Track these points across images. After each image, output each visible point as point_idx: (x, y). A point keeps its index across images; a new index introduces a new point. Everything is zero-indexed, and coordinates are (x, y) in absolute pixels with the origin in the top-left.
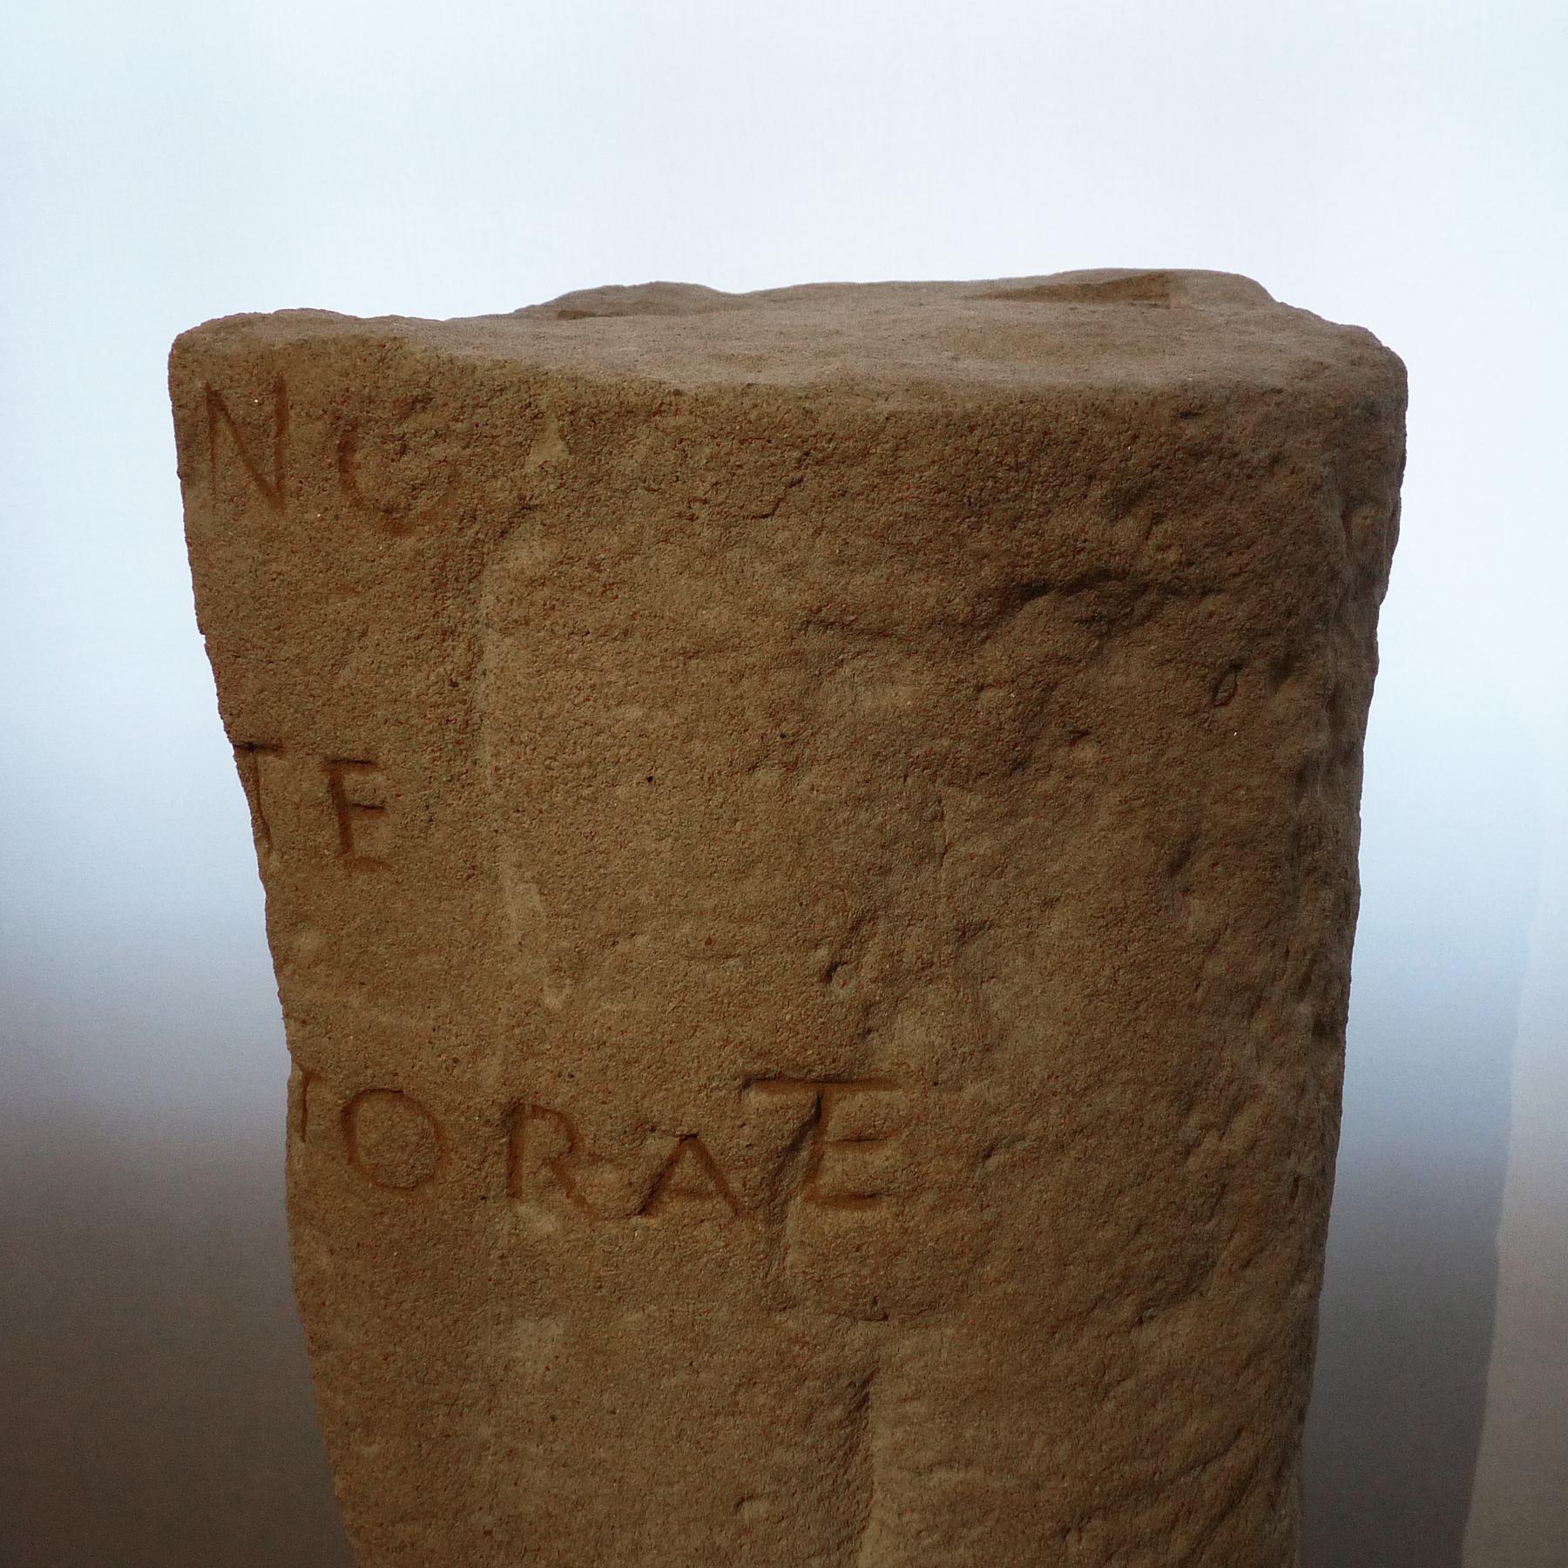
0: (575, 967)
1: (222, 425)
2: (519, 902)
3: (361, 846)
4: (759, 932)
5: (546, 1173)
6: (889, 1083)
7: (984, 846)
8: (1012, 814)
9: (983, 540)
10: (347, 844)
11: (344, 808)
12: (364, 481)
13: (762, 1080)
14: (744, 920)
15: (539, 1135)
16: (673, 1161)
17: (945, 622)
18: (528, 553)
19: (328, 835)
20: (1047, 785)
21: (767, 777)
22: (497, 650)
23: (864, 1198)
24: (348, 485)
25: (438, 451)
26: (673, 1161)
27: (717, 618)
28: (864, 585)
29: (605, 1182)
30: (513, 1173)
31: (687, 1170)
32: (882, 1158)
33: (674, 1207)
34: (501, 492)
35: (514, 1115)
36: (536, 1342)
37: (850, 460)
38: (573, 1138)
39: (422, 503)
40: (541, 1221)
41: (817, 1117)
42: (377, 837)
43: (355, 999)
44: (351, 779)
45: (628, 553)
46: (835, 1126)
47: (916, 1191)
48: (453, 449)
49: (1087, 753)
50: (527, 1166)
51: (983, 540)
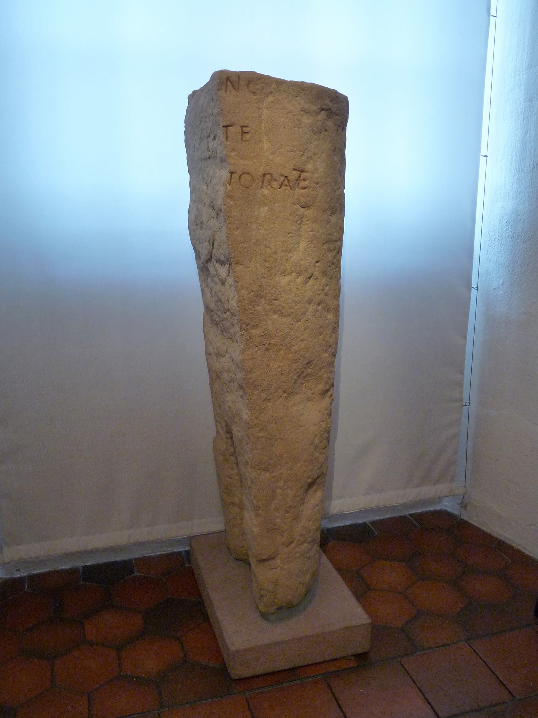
0: (273, 153)
1: (228, 81)
2: (266, 145)
3: (244, 138)
4: (295, 149)
5: (268, 183)
6: (307, 172)
7: (316, 143)
8: (319, 139)
9: (319, 102)
10: (242, 138)
11: (244, 133)
12: (250, 89)
13: (294, 170)
14: (294, 147)
15: (268, 177)
16: (284, 181)
17: (315, 111)
18: (271, 98)
19: (240, 137)
20: (323, 136)
21: (296, 129)
22: (265, 111)
23: (304, 188)
24: (248, 89)
25: (261, 85)
26: (284, 181)
27: (292, 108)
28: (307, 106)
29: (275, 184)
30: (262, 184)
31: (286, 182)
32: (306, 183)
33: (283, 187)
34: (268, 91)
35: (264, 175)
36: (263, 211)
37: (307, 90)
38: (272, 177)
39: (258, 92)
40: (265, 191)
41: (300, 177)
42: (247, 137)
43: (242, 161)
44: (244, 129)
45: (282, 100)
46: (302, 178)
47: (310, 187)
48: (263, 85)
49: (326, 133)
50: (265, 181)
51: (319, 102)
